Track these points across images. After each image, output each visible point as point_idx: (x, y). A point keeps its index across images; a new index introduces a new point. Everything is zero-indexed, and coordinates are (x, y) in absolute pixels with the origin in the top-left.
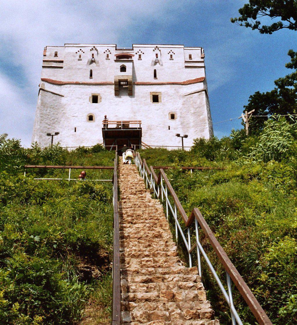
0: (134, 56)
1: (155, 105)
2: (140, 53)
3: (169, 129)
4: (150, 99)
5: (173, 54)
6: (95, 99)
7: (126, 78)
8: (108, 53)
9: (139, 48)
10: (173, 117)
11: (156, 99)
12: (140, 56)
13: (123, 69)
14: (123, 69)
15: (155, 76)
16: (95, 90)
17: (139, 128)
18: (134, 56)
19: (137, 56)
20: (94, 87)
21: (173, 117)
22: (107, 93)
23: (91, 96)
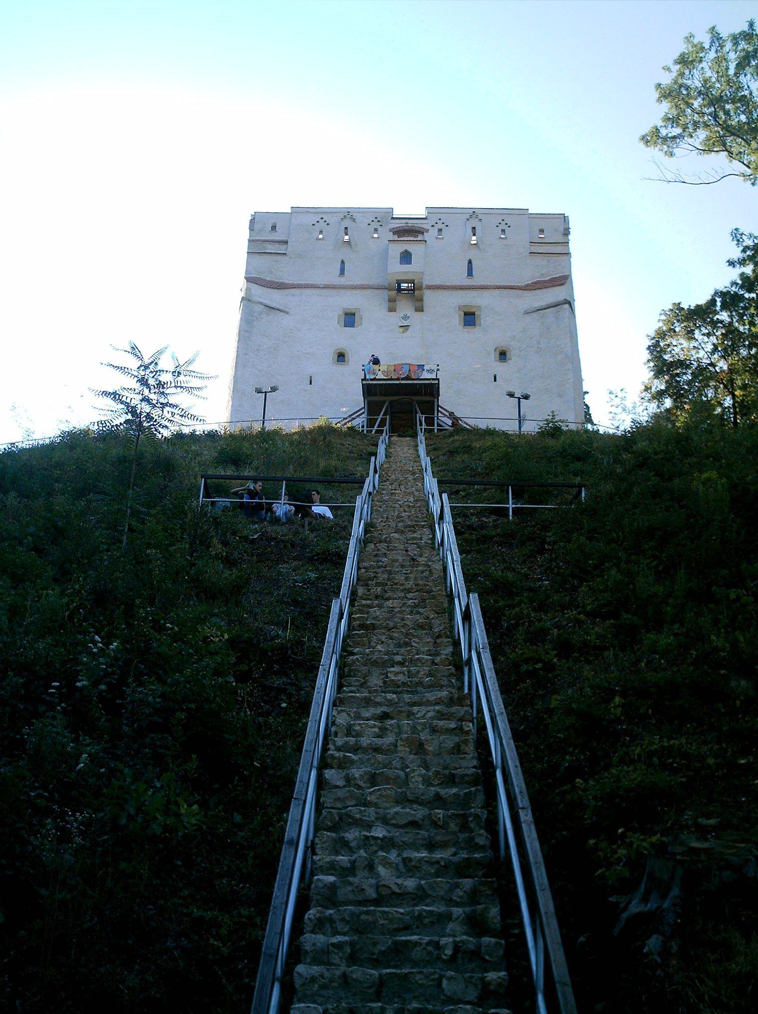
0: (427, 231)
1: (469, 332)
2: (440, 226)
3: (495, 380)
4: (457, 319)
5: (506, 227)
6: (350, 319)
7: (411, 277)
8: (376, 225)
9: (439, 216)
10: (503, 355)
11: (470, 318)
12: (440, 230)
13: (406, 257)
14: (406, 257)
15: (470, 273)
16: (350, 300)
17: (433, 379)
18: (427, 231)
19: (433, 232)
20: (349, 293)
21: (503, 355)
22: (372, 308)
23: (341, 312)
